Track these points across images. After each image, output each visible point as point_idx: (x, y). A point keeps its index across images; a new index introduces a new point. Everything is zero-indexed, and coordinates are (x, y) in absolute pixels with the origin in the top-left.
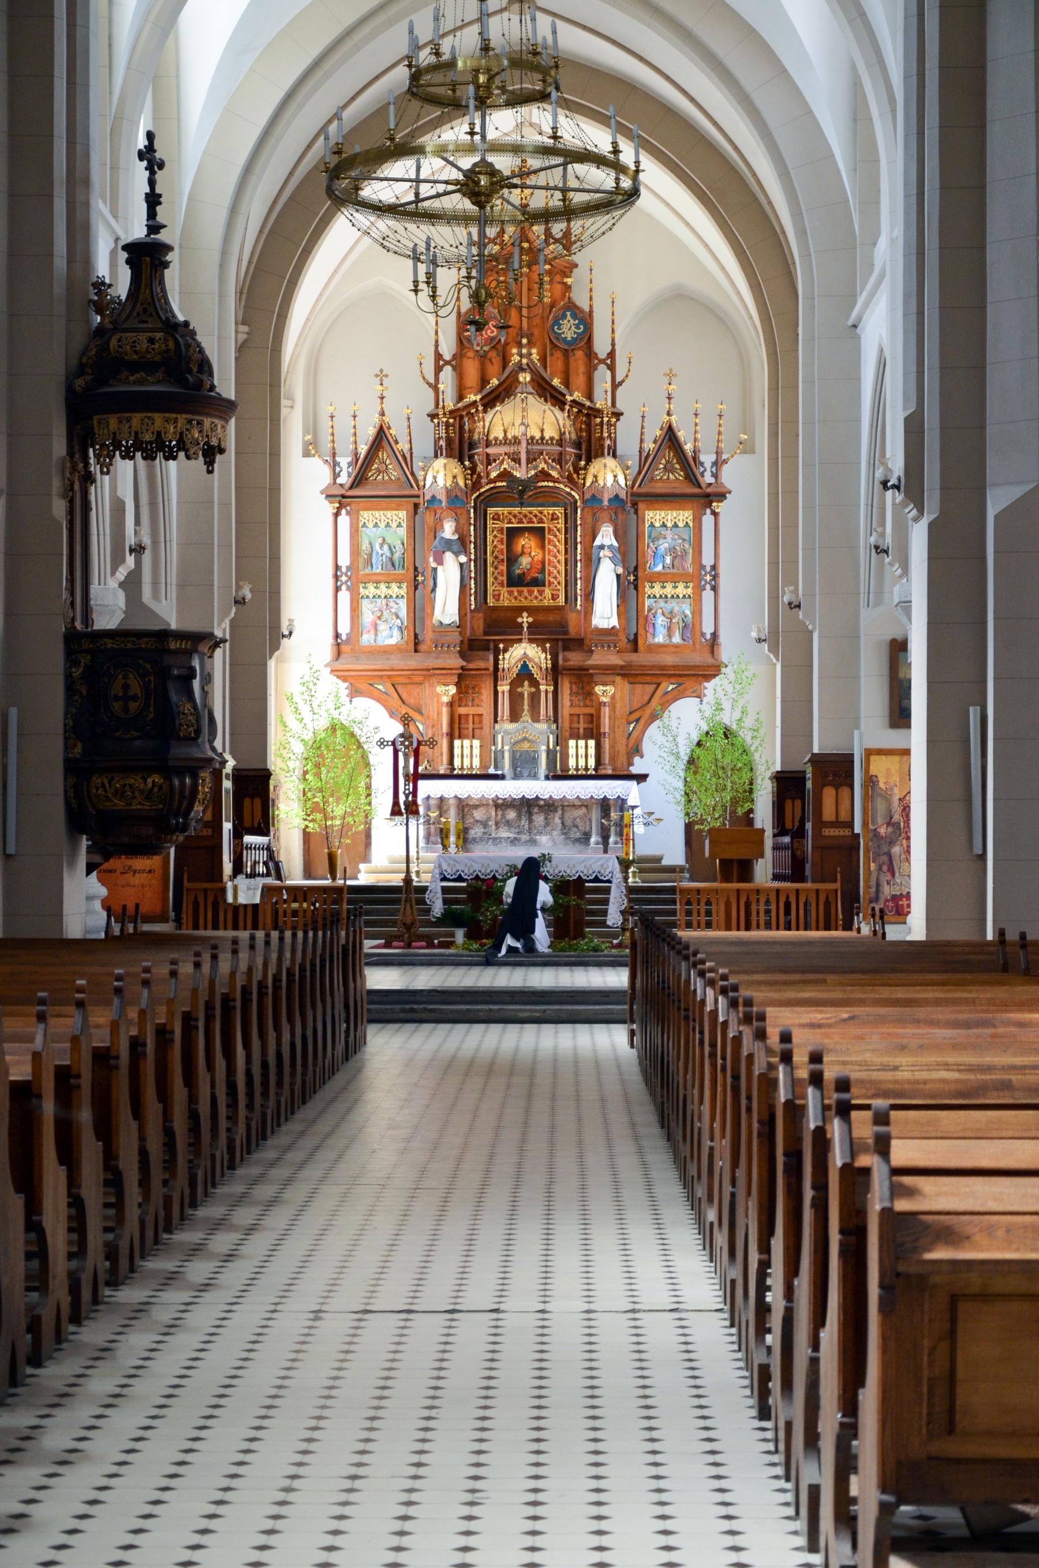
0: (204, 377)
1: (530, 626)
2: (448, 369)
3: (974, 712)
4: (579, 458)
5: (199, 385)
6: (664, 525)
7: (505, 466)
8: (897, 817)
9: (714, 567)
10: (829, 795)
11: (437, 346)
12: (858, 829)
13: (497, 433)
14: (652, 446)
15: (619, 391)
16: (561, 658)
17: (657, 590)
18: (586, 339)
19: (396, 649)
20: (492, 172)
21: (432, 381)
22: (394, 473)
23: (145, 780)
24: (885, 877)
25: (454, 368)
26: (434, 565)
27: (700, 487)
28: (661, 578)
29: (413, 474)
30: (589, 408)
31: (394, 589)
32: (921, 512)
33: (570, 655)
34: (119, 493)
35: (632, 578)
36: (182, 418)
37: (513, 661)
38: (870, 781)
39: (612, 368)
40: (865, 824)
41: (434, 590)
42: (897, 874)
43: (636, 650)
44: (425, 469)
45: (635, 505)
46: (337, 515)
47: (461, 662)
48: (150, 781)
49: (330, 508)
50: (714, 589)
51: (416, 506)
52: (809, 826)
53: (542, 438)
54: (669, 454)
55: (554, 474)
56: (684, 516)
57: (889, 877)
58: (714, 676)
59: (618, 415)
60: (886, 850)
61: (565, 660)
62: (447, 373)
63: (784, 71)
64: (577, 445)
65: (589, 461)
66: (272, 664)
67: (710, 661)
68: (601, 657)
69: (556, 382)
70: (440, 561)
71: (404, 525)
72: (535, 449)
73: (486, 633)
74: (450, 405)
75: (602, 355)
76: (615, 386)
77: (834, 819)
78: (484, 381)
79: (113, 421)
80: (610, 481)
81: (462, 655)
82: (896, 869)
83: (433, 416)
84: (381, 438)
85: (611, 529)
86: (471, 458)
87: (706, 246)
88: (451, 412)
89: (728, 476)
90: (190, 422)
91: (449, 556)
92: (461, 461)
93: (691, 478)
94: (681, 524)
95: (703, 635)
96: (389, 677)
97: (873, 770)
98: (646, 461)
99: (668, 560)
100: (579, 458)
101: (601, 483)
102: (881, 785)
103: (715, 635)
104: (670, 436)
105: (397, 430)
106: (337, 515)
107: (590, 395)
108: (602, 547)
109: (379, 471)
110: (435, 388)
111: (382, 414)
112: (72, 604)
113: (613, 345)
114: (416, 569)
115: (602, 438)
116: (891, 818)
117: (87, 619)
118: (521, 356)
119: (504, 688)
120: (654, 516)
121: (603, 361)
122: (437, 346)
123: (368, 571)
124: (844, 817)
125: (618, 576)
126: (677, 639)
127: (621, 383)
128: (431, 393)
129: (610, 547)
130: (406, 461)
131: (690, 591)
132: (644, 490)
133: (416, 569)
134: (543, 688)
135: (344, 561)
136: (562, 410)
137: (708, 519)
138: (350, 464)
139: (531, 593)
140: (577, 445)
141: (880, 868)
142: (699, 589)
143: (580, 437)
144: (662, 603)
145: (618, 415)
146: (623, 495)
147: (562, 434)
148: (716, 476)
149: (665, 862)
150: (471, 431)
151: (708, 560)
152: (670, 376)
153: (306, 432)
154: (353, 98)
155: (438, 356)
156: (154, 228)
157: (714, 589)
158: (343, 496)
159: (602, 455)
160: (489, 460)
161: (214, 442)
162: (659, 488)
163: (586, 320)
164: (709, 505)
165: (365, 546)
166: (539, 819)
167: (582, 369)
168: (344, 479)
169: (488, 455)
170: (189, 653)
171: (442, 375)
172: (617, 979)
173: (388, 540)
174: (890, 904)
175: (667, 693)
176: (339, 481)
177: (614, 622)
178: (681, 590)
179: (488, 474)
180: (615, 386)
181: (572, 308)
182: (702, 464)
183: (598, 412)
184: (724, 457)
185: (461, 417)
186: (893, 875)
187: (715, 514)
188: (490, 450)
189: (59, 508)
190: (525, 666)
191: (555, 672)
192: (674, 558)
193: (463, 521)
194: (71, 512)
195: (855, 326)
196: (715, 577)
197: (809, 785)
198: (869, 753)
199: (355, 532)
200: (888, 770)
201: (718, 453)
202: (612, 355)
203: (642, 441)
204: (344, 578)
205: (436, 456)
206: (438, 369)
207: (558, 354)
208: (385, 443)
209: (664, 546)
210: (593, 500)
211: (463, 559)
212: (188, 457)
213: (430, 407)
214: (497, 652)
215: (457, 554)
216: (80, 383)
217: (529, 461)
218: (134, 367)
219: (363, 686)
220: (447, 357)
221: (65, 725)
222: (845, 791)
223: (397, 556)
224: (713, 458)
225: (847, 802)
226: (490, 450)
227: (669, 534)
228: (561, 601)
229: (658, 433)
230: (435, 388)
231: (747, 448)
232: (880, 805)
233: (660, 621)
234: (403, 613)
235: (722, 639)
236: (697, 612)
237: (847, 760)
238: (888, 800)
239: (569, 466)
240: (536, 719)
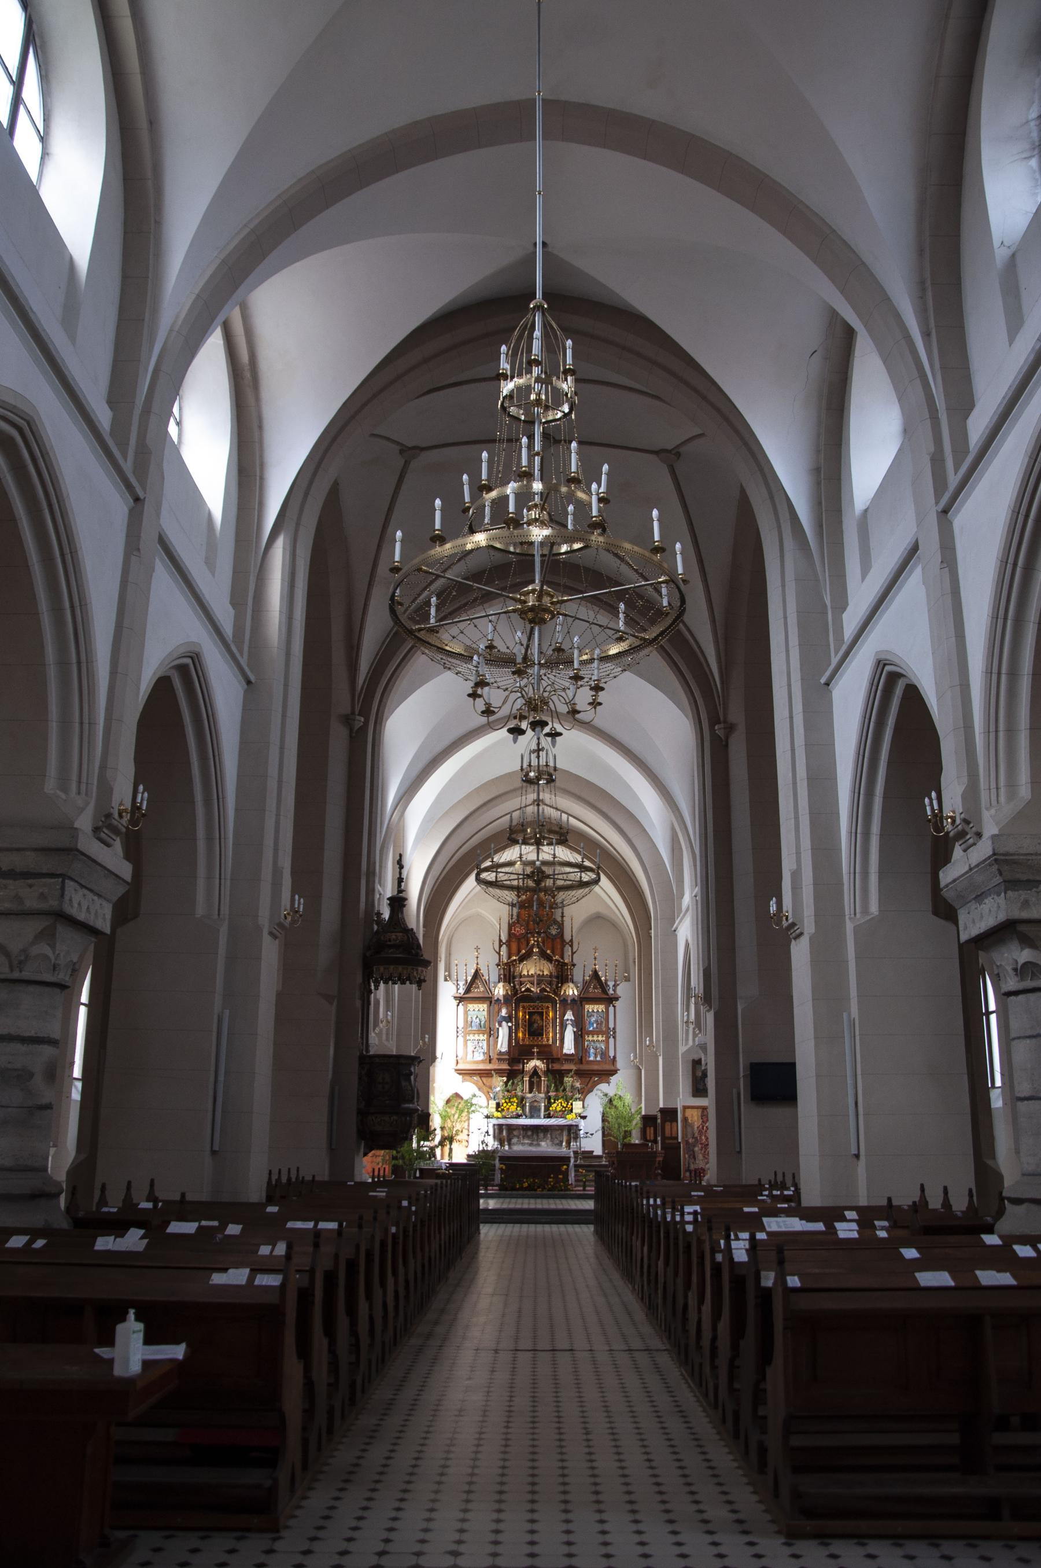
0: (419, 951)
1: (537, 1052)
2: (504, 946)
3: (735, 1091)
4: (558, 983)
5: (417, 954)
6: (593, 1011)
7: (528, 986)
8: (696, 1135)
9: (614, 1029)
10: (668, 1125)
11: (500, 936)
12: (680, 1140)
13: (525, 973)
14: (588, 978)
15: (575, 955)
16: (550, 1066)
17: (590, 1038)
18: (561, 934)
19: (483, 1062)
20: (543, 872)
21: (498, 951)
22: (482, 989)
23: (390, 1117)
25: (507, 946)
26: (497, 1026)
27: (608, 994)
28: (593, 1033)
29: (489, 989)
30: (562, 963)
31: (481, 1037)
32: (711, 1008)
33: (554, 1065)
34: (378, 997)
35: (580, 1033)
36: (410, 968)
37: (531, 1068)
38: (685, 1119)
39: (571, 946)
40: (683, 1138)
41: (497, 1038)
43: (581, 1063)
44: (495, 987)
45: (581, 1002)
46: (458, 1005)
47: (508, 1067)
48: (392, 1118)
49: (455, 1002)
50: (614, 1037)
51: (491, 1002)
52: (659, 1139)
53: (543, 975)
54: (595, 982)
55: (548, 989)
56: (601, 1008)
57: (693, 1160)
58: (614, 1074)
59: (574, 965)
61: (552, 1067)
62: (504, 948)
63: (645, 830)
64: (557, 977)
65: (562, 984)
66: (431, 1068)
67: (612, 1068)
68: (566, 1067)
69: (548, 952)
70: (500, 1025)
71: (486, 1010)
72: (540, 979)
73: (519, 1055)
74: (505, 961)
75: (568, 941)
76: (573, 953)
77: (670, 1136)
78: (519, 951)
79: (382, 969)
80: (571, 993)
81: (509, 1064)
83: (498, 965)
84: (477, 975)
85: (571, 1013)
86: (514, 983)
87: (610, 897)
88: (506, 964)
89: (620, 991)
90: (413, 969)
91: (504, 1023)
92: (510, 984)
93: (604, 991)
94: (600, 1010)
95: (610, 1057)
96: (479, 1074)
98: (586, 985)
99: (595, 1025)
100: (558, 983)
101: (567, 993)
102: (690, 1121)
103: (615, 1057)
104: (595, 975)
105: (484, 971)
106: (458, 1005)
107: (562, 958)
108: (568, 1020)
109: (475, 988)
110: (499, 953)
111: (477, 964)
112: (362, 1043)
113: (572, 936)
114: (490, 1028)
115: (568, 975)
117: (367, 1050)
118: (535, 941)
119: (526, 1079)
120: (589, 1008)
121: (568, 943)
122: (500, 936)
123: (470, 1029)
124: (674, 1135)
125: (574, 1032)
126: (598, 1059)
127: (575, 952)
128: (497, 955)
129: (571, 1020)
130: (486, 983)
131: (604, 1039)
132: (585, 996)
133: (490, 1028)
134: (543, 1079)
135: (461, 1025)
136: (551, 963)
137: (611, 1009)
138: (464, 985)
139: (538, 1038)
140: (557, 977)
141: (689, 1157)
142: (608, 1038)
143: (558, 974)
144: (592, 1044)
145: (574, 965)
146: (576, 999)
147: (551, 973)
148: (614, 990)
149: (594, 1154)
150: (514, 972)
151: (611, 1026)
152: (596, 949)
153: (445, 971)
154: (470, 838)
155: (500, 941)
156: (400, 891)
157: (614, 1037)
158: (461, 998)
159: (568, 982)
160: (521, 983)
161: (422, 978)
162: (591, 995)
163: (561, 926)
164: (612, 1003)
165: (469, 1019)
166: (541, 1135)
167: (559, 947)
168: (462, 991)
169: (521, 981)
170: (410, 1065)
171: (502, 948)
172: (589, 1205)
173: (479, 1016)
175: (595, 1081)
176: (459, 991)
177: (573, 1051)
178: (600, 1038)
179: (521, 989)
180: (573, 953)
181: (555, 922)
182: (609, 986)
183: (566, 964)
184: (618, 983)
185: (510, 966)
187: (614, 1006)
188: (521, 979)
189: (358, 1004)
190: (535, 1070)
191: (548, 1072)
192: (597, 1024)
193: (510, 1009)
194: (363, 1006)
195: (675, 931)
196: (615, 1033)
197: (659, 1121)
198: (685, 1108)
199: (466, 1013)
200: (692, 1115)
201: (615, 981)
202: (571, 941)
203: (584, 976)
204: (460, 1032)
205: (499, 982)
206: (500, 946)
207: (550, 940)
208: (478, 977)
209: (593, 1019)
210: (564, 1001)
211: (510, 1024)
212: (411, 983)
213: (497, 961)
214: (524, 1064)
215: (507, 1022)
216: (368, 954)
217: (538, 984)
218: (390, 947)
219: (467, 1077)
220: (504, 941)
221: (358, 1094)
222: (674, 1124)
223: (482, 1023)
224: (613, 983)
225: (675, 1128)
226: (521, 979)
227: (595, 1014)
228: (550, 1042)
229: (591, 973)
230: (499, 953)
231: (627, 979)
232: (689, 1130)
233: (592, 1051)
234: (485, 1047)
235: (618, 1059)
236: (607, 1047)
237: (674, 1111)
239: (554, 987)
240: (540, 1092)
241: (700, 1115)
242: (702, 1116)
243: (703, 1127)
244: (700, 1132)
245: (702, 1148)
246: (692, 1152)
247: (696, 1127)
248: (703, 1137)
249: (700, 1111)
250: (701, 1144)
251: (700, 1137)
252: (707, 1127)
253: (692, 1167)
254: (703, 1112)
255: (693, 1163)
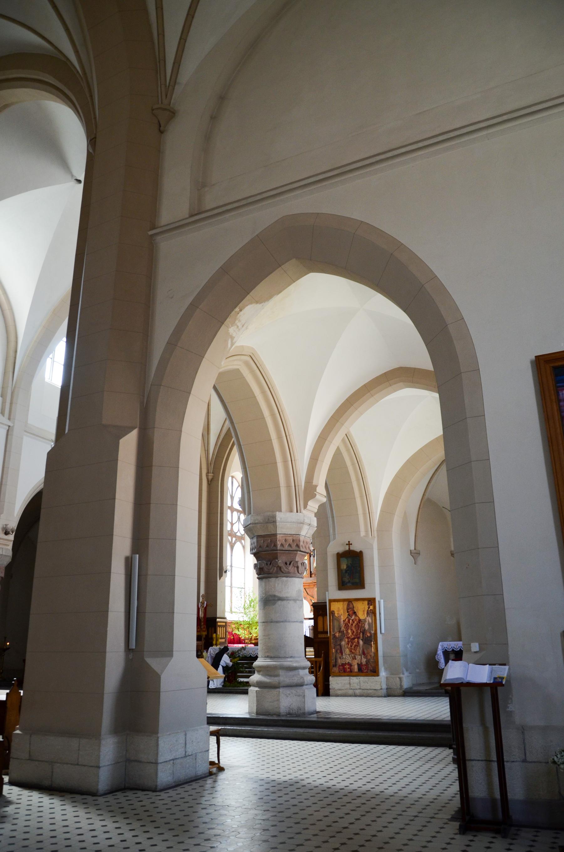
8: (343, 629)
24: (339, 655)
38: (332, 613)
42: (344, 654)
57: (340, 655)
60: (339, 643)
77: (322, 630)
82: (343, 651)
97: (332, 609)
102: (336, 615)
116: (340, 629)
141: (336, 651)
174: (341, 667)
186: (342, 655)
198: (331, 601)
200: (339, 608)
232: (336, 624)
238: (339, 622)
241: (346, 607)
242: (348, 609)
243: (349, 620)
244: (347, 626)
245: (348, 642)
246: (338, 647)
247: (342, 620)
248: (350, 631)
249: (346, 603)
250: (348, 638)
251: (347, 631)
252: (353, 620)
253: (340, 662)
254: (348, 605)
255: (340, 658)
